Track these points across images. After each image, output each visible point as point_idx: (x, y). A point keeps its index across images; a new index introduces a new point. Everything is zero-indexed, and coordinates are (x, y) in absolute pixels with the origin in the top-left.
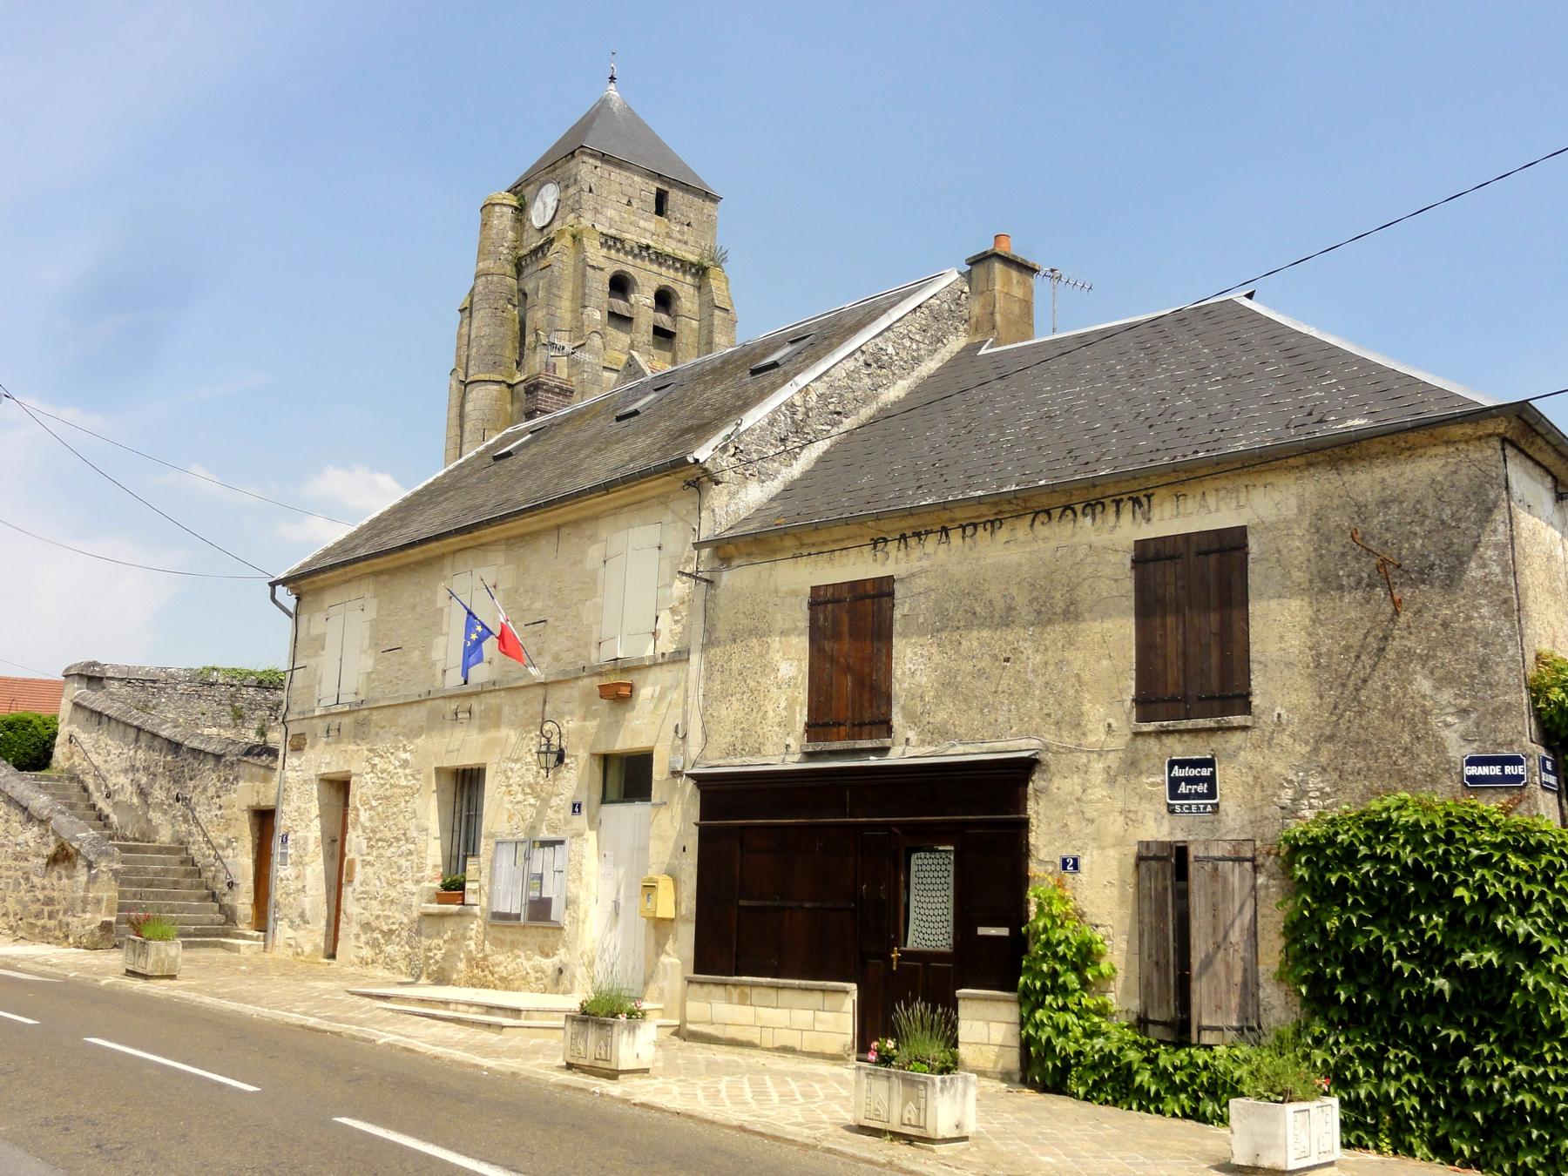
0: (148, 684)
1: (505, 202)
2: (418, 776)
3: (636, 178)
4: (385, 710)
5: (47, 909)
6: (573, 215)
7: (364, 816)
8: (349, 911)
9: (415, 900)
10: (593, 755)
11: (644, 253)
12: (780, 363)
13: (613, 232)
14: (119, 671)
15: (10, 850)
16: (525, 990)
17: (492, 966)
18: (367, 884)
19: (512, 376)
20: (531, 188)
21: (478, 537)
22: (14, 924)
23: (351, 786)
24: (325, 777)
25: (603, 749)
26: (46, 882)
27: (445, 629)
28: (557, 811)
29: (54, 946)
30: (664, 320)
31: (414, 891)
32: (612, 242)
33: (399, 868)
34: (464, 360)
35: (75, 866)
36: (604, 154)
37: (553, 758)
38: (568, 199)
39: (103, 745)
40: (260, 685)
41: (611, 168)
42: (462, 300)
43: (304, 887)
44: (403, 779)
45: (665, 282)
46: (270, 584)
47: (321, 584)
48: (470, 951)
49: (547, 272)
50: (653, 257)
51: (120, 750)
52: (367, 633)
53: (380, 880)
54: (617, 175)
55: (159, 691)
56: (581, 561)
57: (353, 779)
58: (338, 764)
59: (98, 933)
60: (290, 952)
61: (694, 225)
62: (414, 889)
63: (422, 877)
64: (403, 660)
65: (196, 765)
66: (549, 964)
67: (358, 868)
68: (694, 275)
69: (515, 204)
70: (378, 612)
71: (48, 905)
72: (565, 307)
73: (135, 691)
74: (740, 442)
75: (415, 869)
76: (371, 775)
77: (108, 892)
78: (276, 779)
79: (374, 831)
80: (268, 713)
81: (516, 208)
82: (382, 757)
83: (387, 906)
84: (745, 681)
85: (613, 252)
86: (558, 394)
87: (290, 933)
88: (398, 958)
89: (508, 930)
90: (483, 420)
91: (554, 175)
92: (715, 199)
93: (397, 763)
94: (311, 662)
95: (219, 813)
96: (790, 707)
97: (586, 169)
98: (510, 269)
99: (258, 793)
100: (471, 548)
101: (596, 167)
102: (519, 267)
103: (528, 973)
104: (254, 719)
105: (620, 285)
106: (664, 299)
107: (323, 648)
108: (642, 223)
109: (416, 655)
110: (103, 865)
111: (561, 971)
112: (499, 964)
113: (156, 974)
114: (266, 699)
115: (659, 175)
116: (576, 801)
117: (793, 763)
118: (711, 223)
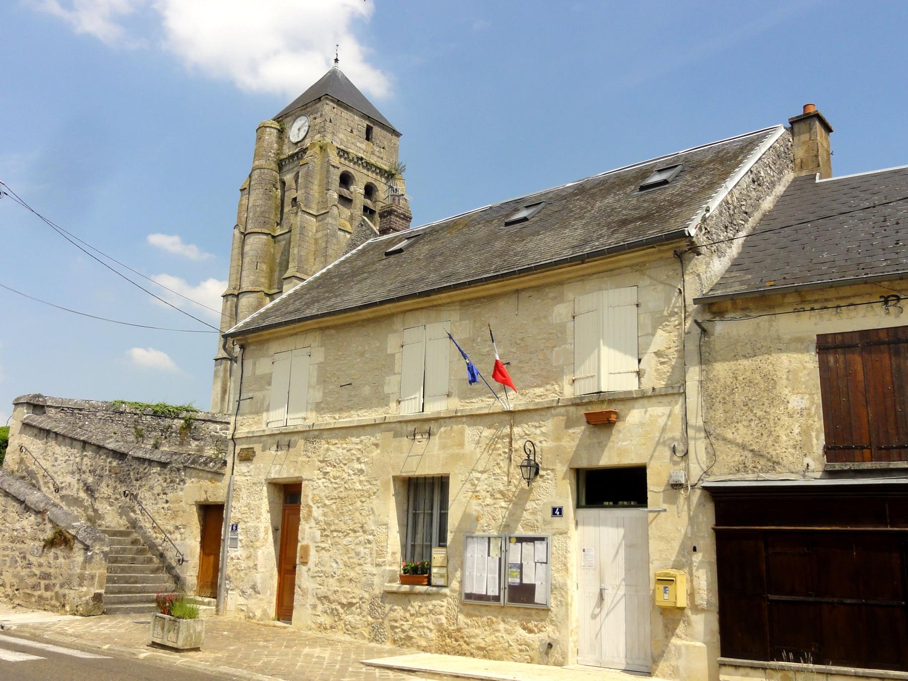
0: (76, 411)
1: (272, 126)
2: (375, 482)
3: (356, 117)
4: (337, 431)
5: (43, 582)
6: (319, 135)
7: (317, 512)
8: (304, 586)
9: (376, 580)
10: (571, 468)
11: (360, 162)
12: (669, 180)
13: (342, 147)
14: (56, 402)
15: (7, 535)
16: (508, 660)
17: (467, 637)
18: (324, 566)
19: (274, 231)
20: (288, 119)
21: (435, 300)
22: (11, 594)
23: (303, 489)
24: (274, 481)
25: (584, 464)
26: (42, 560)
27: (397, 369)
28: (533, 513)
29: (50, 613)
31: (374, 572)
32: (343, 153)
33: (358, 554)
34: (244, 220)
35: (71, 549)
36: (339, 101)
37: (534, 470)
39: (51, 454)
40: (155, 414)
41: (342, 110)
42: (243, 182)
43: (256, 565)
44: (358, 484)
46: (223, 336)
47: (268, 337)
48: (441, 624)
50: (365, 165)
51: (67, 458)
52: (315, 373)
53: (337, 563)
54: (346, 114)
55: (84, 416)
56: (545, 317)
57: (304, 483)
58: (288, 471)
59: (91, 603)
60: (242, 615)
61: (386, 148)
62: (374, 570)
63: (384, 562)
64: (353, 393)
65: (141, 469)
66: (536, 639)
67: (312, 552)
69: (279, 127)
70: (326, 358)
71: (44, 579)
72: (315, 189)
73: (67, 416)
74: (708, 225)
75: (375, 555)
76: (324, 480)
77: (99, 569)
78: (226, 480)
79: (328, 524)
80: (160, 434)
81: (279, 131)
82: (335, 466)
83: (345, 583)
84: (752, 411)
85: (343, 159)
86: (403, 219)
87: (241, 600)
88: (360, 626)
89: (484, 609)
92: (398, 135)
93: (351, 472)
94: (258, 395)
95: (166, 506)
96: (806, 431)
97: (328, 108)
98: (274, 166)
99: (206, 492)
100: (423, 308)
101: (334, 108)
102: (281, 165)
103: (511, 646)
104: (150, 438)
105: (346, 180)
106: (369, 191)
107: (269, 384)
108: (358, 144)
109: (367, 390)
110: (97, 548)
111: (550, 646)
112: (477, 636)
113: (186, 648)
114: (158, 424)
115: (369, 117)
116: (555, 506)
117: (815, 479)
118: (395, 149)
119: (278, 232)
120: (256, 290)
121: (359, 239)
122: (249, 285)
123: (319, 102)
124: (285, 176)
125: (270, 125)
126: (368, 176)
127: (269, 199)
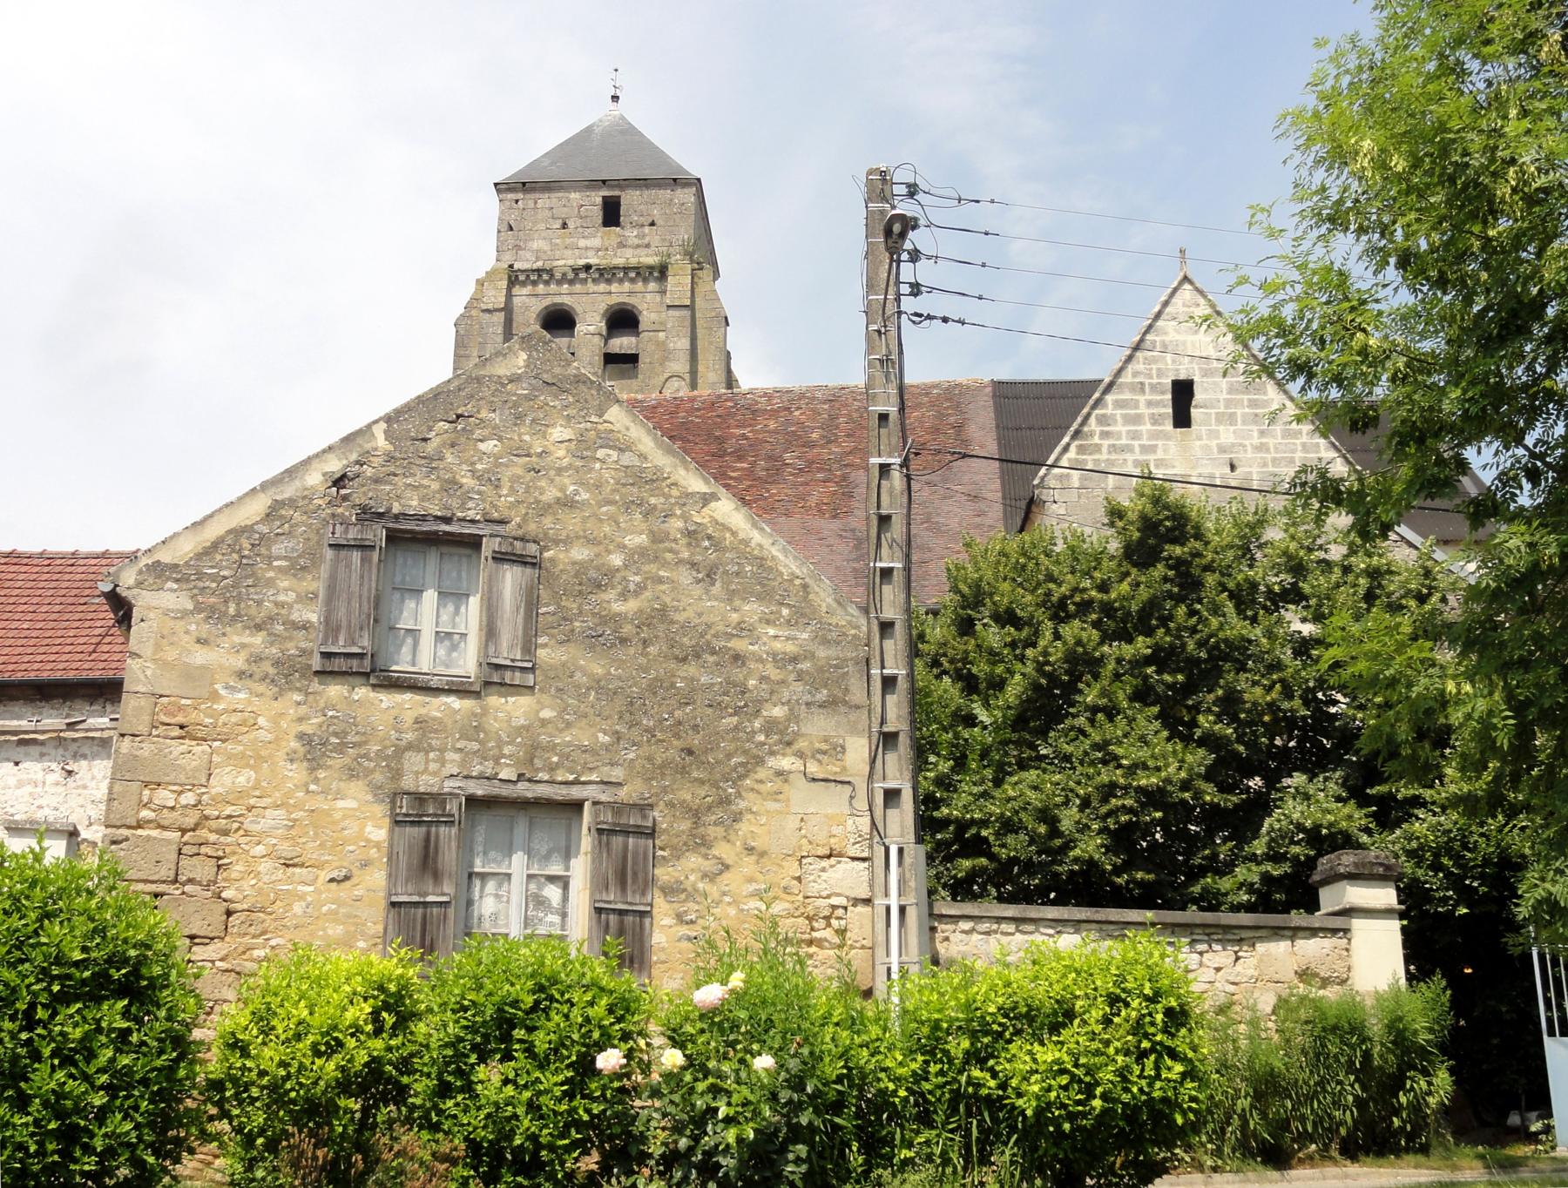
3: (573, 195)
11: (583, 275)
13: (539, 264)
30: (622, 344)
36: (524, 184)
41: (537, 195)
45: (615, 300)
54: (544, 200)
61: (659, 222)
85: (541, 286)
101: (517, 201)
106: (622, 320)
108: (582, 243)
115: (604, 182)
126: (610, 293)
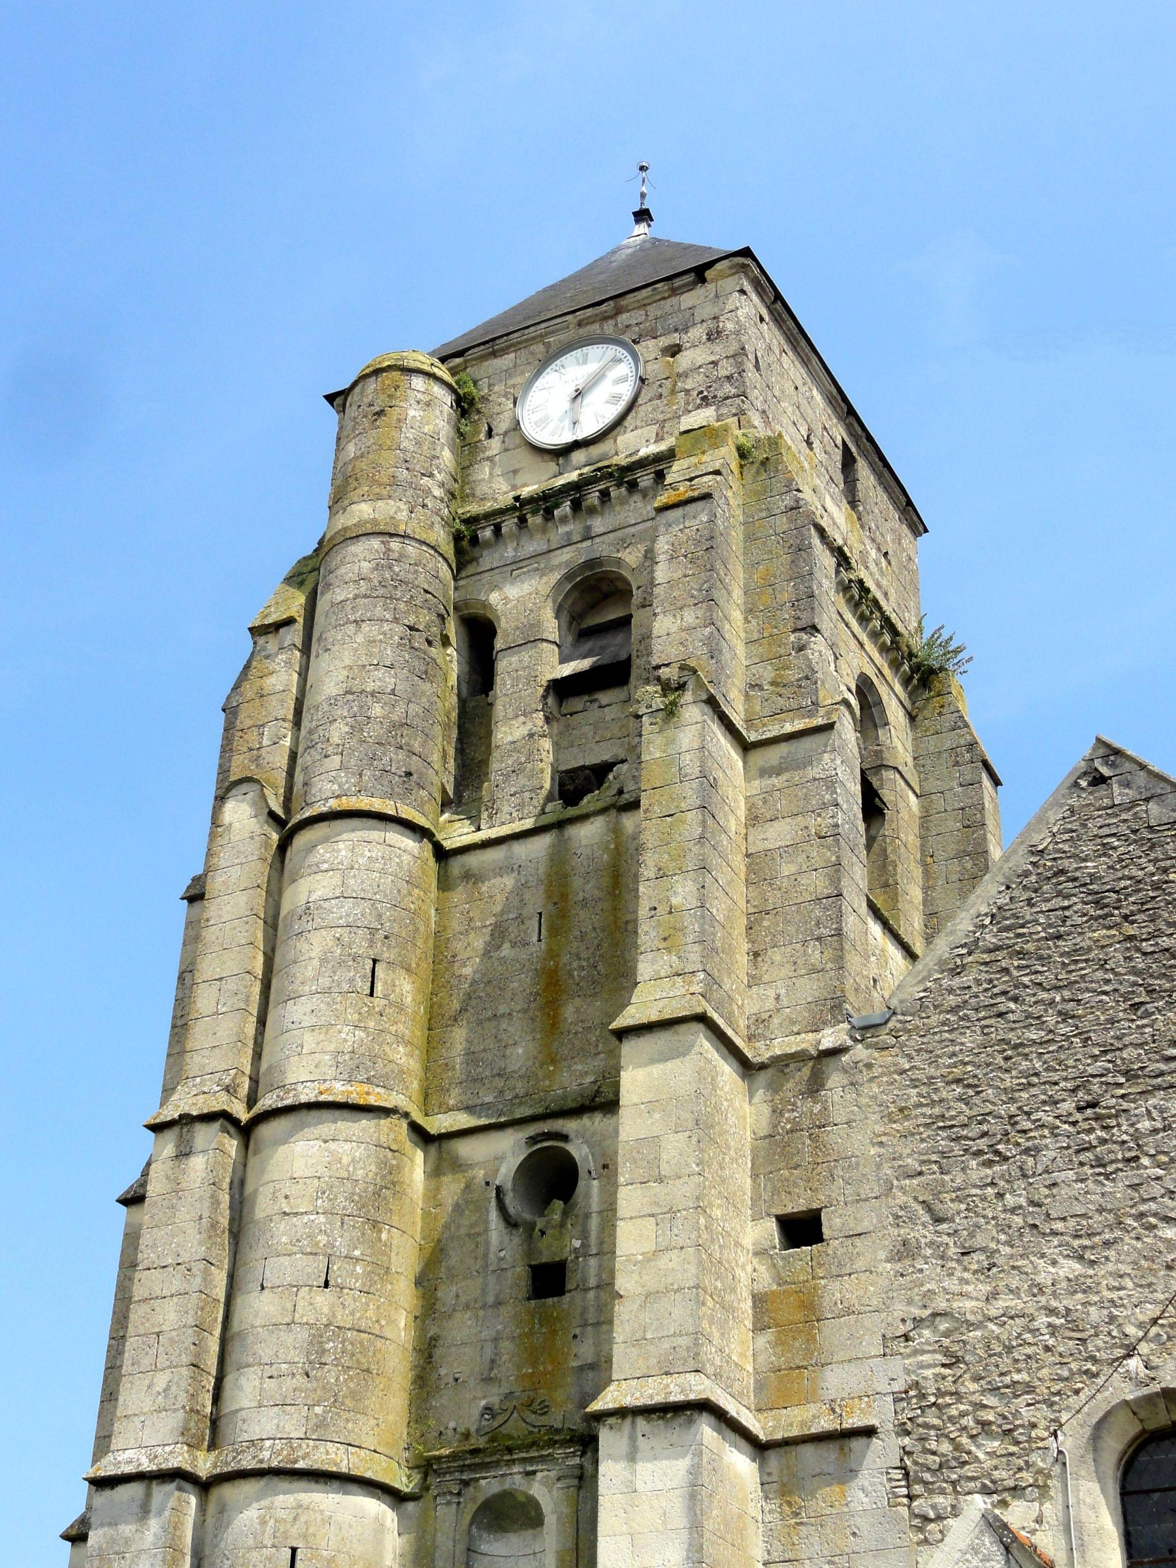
38: (685, 375)
49: (700, 515)
68: (906, 682)
90: (373, 931)
91: (609, 328)
92: (917, 526)
98: (441, 537)
119: (458, 833)
120: (372, 1100)
121: (1087, 849)
122: (331, 1073)
123: (691, 286)
124: (495, 587)
125: (426, 368)
127: (425, 676)
